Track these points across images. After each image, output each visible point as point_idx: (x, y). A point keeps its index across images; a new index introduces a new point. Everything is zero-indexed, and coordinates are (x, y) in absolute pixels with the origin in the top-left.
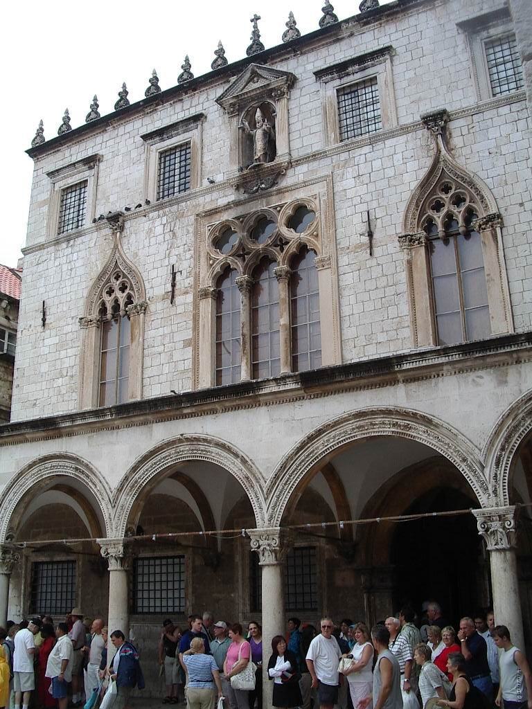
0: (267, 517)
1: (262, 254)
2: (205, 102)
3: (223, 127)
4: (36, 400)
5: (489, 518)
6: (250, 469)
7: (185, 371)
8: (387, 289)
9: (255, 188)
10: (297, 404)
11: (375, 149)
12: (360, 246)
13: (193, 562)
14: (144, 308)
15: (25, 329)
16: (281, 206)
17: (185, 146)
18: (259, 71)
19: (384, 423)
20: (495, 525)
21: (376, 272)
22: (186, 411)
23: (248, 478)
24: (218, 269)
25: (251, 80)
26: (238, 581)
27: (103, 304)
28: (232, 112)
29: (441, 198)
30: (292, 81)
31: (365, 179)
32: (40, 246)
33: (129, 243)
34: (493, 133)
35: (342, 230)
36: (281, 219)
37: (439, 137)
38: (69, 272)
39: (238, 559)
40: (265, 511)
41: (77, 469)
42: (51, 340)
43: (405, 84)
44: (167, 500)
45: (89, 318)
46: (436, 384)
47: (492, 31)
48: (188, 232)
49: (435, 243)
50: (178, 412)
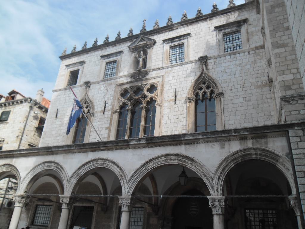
0: (127, 191)
1: (137, 103)
2: (124, 47)
4: (49, 143)
5: (214, 201)
6: (123, 172)
9: (138, 77)
10: (143, 149)
12: (172, 100)
13: (97, 209)
14: (93, 114)
16: (146, 84)
17: (115, 62)
18: (144, 38)
19: (175, 159)
20: (217, 204)
21: (177, 109)
22: (102, 148)
23: (121, 176)
24: (121, 104)
25: (141, 41)
26: (113, 218)
28: (133, 51)
29: (202, 86)
30: (154, 43)
31: (176, 77)
34: (223, 65)
36: (145, 89)
37: (204, 65)
39: (114, 209)
40: (126, 189)
41: (57, 167)
42: (58, 122)
44: (90, 184)
46: (197, 146)
47: (227, 30)
48: (112, 90)
49: (199, 102)
50: (99, 149)
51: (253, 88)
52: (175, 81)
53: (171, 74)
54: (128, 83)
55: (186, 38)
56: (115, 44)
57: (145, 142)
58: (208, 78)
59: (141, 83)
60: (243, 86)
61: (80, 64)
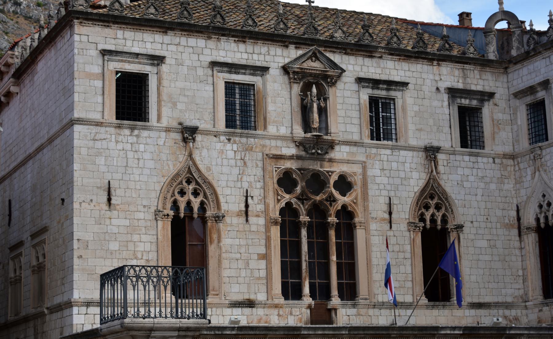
3: (284, 86)
7: (259, 278)
8: (399, 253)
9: (313, 151)
11: (394, 153)
12: (383, 220)
15: (84, 201)
16: (332, 172)
18: (318, 55)
24: (283, 205)
25: (310, 58)
27: (175, 203)
31: (387, 172)
32: (97, 122)
33: (201, 156)
35: (373, 204)
36: (332, 182)
37: (433, 162)
38: (136, 161)
42: (117, 222)
43: (413, 114)
45: (166, 212)
47: (463, 101)
48: (257, 166)
51: (499, 225)
52: (385, 180)
53: (377, 162)
54: (293, 159)
55: (399, 90)
56: (244, 37)
57: (461, 332)
58: (439, 190)
59: (321, 167)
60: (487, 219)
61: (152, 62)
